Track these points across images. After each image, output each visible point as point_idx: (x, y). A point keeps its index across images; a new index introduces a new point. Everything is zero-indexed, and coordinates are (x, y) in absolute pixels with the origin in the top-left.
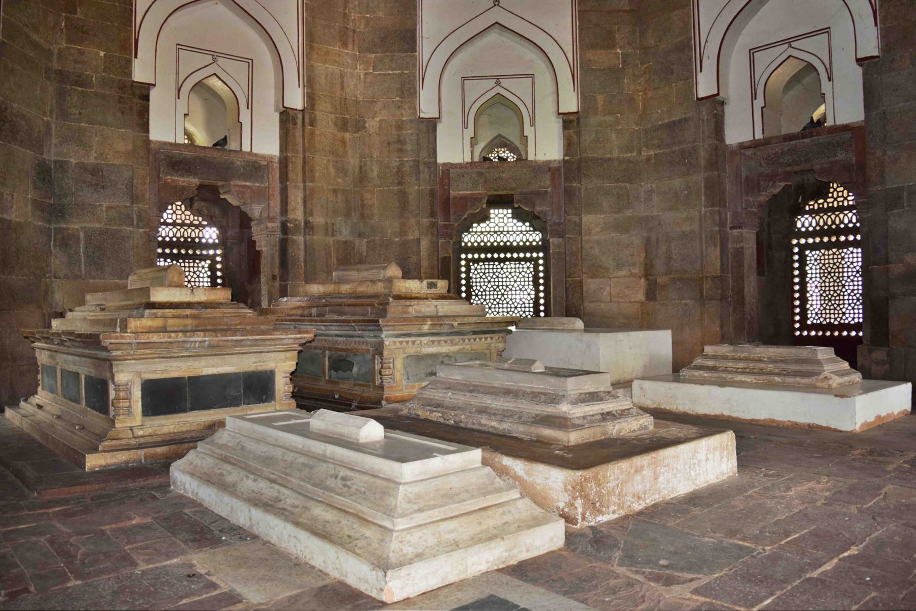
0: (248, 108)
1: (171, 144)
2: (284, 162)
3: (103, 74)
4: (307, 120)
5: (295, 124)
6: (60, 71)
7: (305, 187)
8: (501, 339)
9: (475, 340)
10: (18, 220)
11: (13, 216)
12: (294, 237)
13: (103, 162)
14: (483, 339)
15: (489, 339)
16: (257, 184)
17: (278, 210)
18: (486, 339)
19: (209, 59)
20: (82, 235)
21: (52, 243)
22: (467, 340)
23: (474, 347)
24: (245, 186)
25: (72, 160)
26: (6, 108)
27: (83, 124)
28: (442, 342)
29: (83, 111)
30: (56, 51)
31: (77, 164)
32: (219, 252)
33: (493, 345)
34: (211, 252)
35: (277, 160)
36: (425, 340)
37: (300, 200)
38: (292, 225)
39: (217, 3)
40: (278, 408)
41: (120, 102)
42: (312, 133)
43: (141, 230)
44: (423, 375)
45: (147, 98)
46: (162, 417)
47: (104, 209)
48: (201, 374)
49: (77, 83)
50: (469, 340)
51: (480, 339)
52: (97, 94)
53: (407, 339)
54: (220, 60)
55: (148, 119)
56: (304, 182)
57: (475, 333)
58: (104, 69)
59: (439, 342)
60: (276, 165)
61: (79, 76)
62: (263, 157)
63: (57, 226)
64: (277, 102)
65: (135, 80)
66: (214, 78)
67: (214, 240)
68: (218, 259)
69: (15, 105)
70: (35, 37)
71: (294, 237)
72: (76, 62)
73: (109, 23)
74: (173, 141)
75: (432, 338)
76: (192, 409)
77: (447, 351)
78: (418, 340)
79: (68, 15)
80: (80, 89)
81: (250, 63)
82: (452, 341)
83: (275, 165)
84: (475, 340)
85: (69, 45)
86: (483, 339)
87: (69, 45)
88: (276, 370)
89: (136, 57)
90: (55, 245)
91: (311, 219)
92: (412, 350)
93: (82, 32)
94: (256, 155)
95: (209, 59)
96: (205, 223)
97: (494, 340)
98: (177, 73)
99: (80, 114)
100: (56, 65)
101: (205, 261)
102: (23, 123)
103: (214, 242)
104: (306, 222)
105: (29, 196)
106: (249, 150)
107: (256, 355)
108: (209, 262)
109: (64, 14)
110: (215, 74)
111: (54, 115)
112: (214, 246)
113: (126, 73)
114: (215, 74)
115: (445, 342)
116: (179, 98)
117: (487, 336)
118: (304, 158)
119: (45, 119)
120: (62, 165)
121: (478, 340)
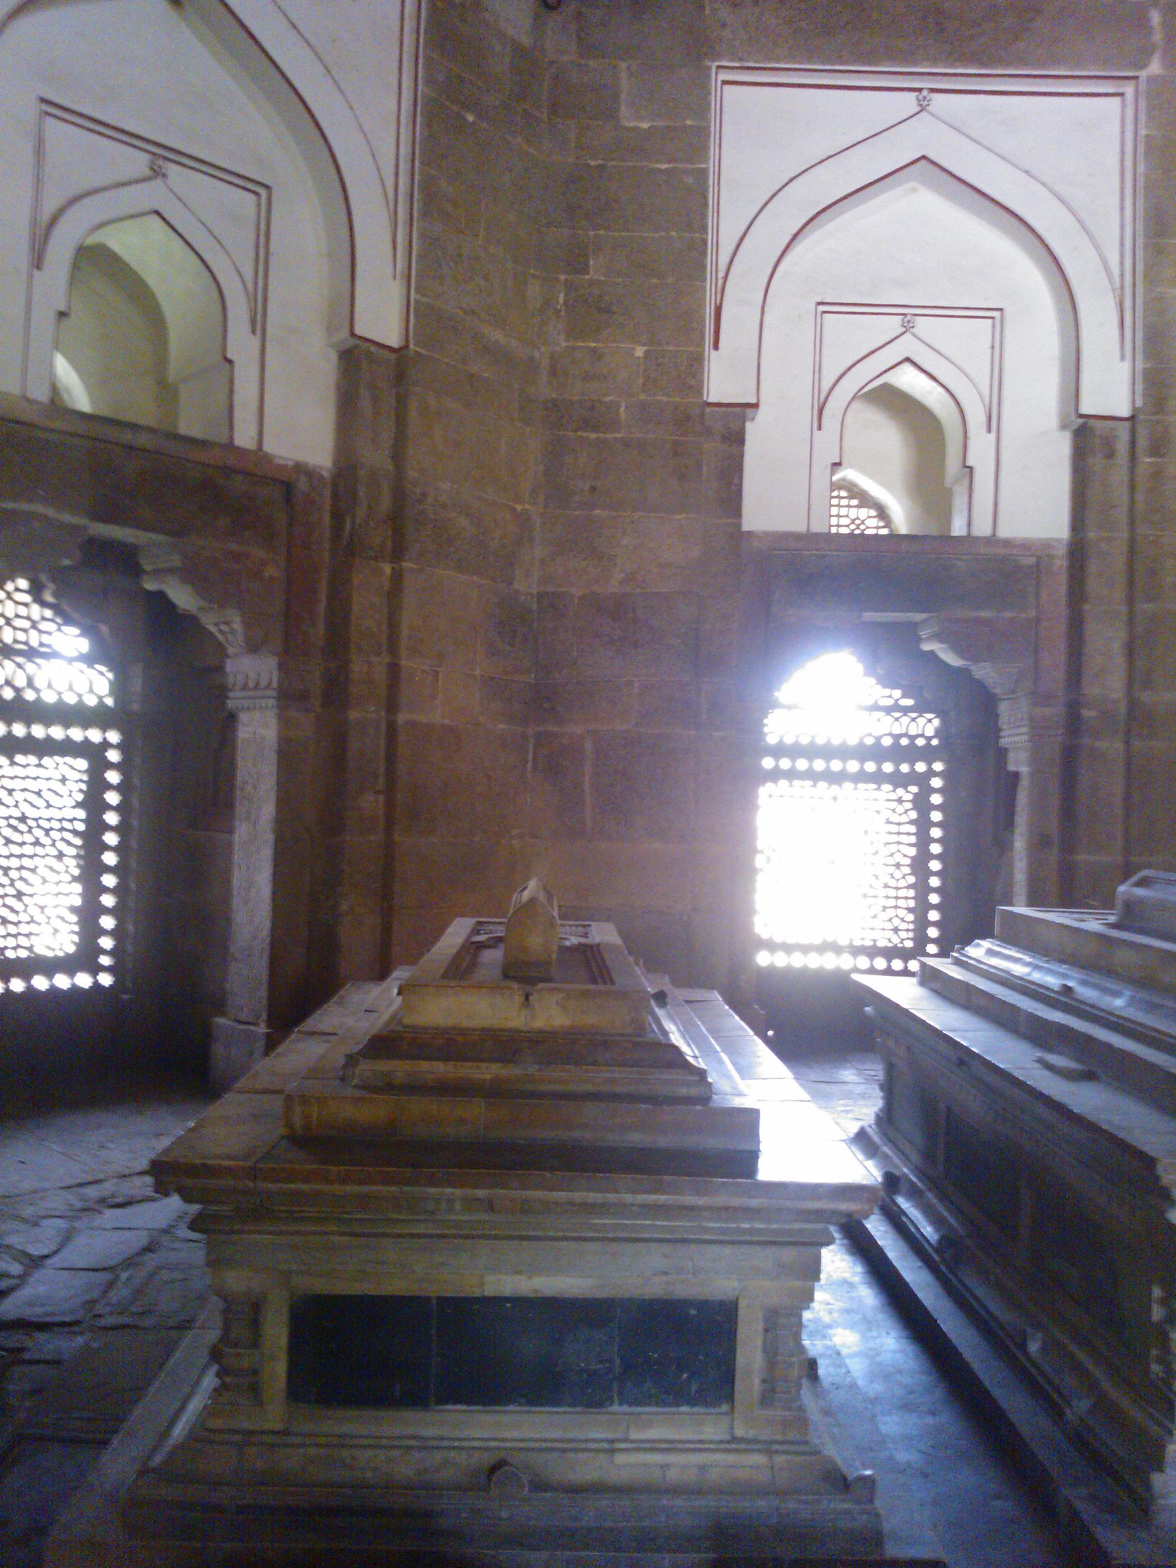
0: (989, 431)
1: (797, 536)
2: (1078, 551)
3: (642, 397)
4: (1142, 442)
5: (1111, 455)
6: (554, 401)
7: (1131, 614)
10: (447, 722)
11: (437, 716)
12: (1099, 744)
13: (639, 590)
16: (1008, 614)
17: (1060, 675)
19: (893, 324)
20: (589, 746)
21: (529, 766)
24: (978, 621)
25: (573, 591)
26: (424, 495)
27: (597, 512)
29: (598, 484)
30: (545, 363)
31: (581, 598)
32: (938, 766)
34: (921, 767)
35: (1061, 551)
37: (1117, 646)
38: (1093, 713)
39: (914, 190)
40: (739, 1433)
41: (676, 454)
42: (1157, 474)
45: (737, 439)
46: (353, 1412)
47: (636, 690)
48: (477, 1293)
49: (586, 424)
52: (627, 444)
54: (923, 325)
55: (740, 486)
56: (1131, 600)
58: (644, 384)
60: (1061, 563)
61: (592, 408)
62: (1026, 546)
63: (541, 729)
64: (1063, 401)
65: (712, 399)
66: (907, 368)
67: (929, 739)
68: (936, 783)
69: (445, 486)
70: (498, 336)
71: (1099, 744)
72: (587, 378)
73: (655, 281)
74: (800, 527)
76: (441, 1401)
79: (570, 278)
80: (593, 436)
81: (995, 314)
83: (1058, 562)
85: (572, 343)
87: (572, 343)
89: (716, 347)
90: (535, 767)
91: (1145, 697)
93: (599, 310)
94: (1007, 543)
95: (893, 324)
96: (909, 702)
98: (818, 369)
99: (593, 489)
100: (544, 389)
101: (905, 787)
102: (463, 522)
103: (928, 745)
104: (1133, 705)
105: (477, 672)
106: (964, 533)
107: (667, 1249)
108: (914, 789)
109: (562, 277)
110: (908, 360)
111: (541, 499)
112: (928, 754)
113: (691, 387)
114: (908, 360)
116: (820, 428)
118: (1132, 542)
119: (519, 507)
120: (552, 603)
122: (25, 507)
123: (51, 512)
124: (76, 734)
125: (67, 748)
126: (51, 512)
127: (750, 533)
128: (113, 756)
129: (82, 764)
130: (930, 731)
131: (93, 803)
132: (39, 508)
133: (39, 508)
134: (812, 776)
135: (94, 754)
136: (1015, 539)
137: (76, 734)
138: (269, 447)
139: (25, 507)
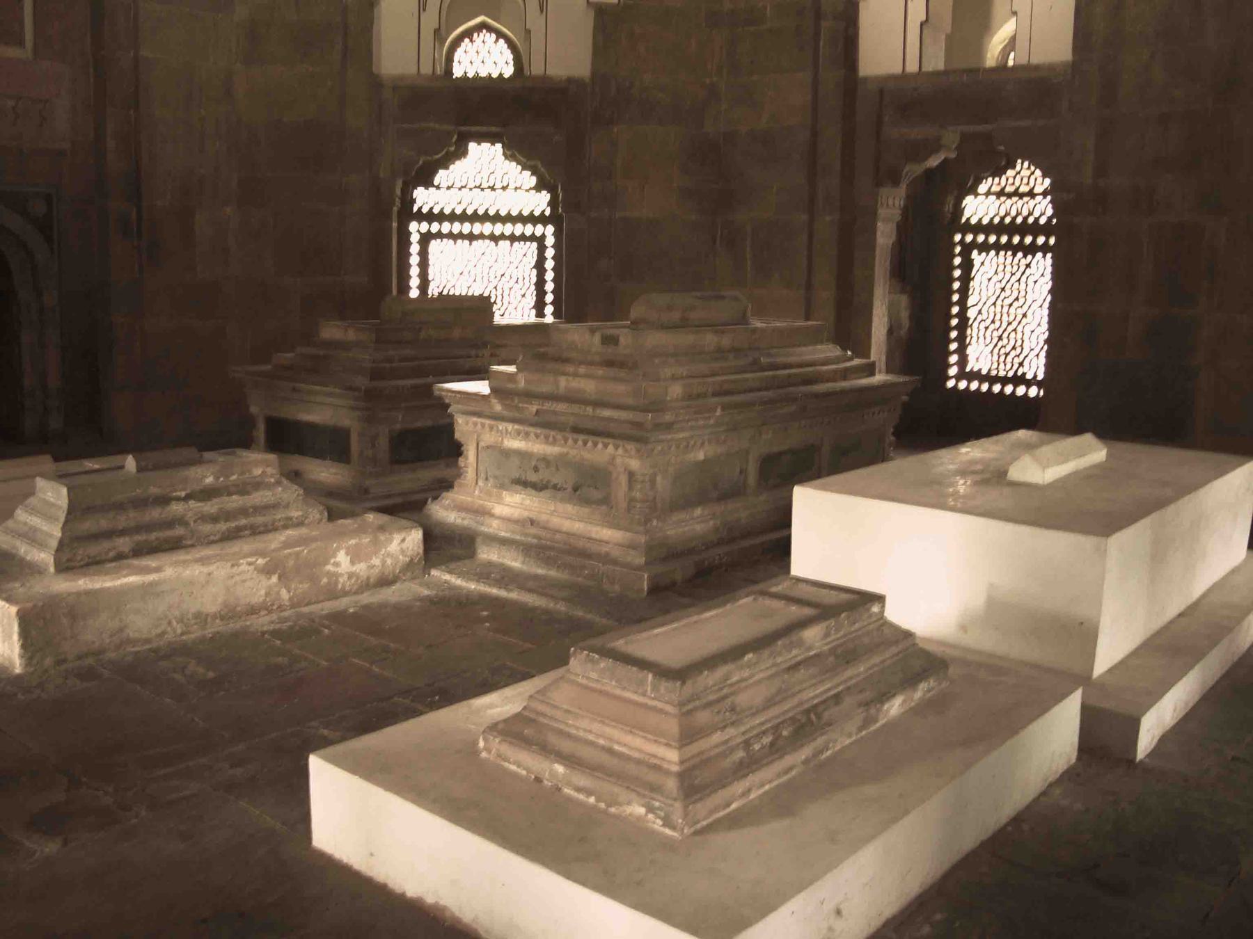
8: (633, 453)
9: (585, 443)
14: (600, 446)
15: (611, 448)
18: (606, 446)
22: (570, 441)
23: (587, 455)
28: (532, 435)
33: (619, 460)
36: (510, 427)
43: (828, 218)
44: (506, 481)
50: (576, 441)
51: (595, 445)
53: (475, 419)
57: (576, 430)
59: (527, 434)
62: (1051, 68)
74: (898, 69)
75: (516, 427)
77: (541, 452)
78: (502, 426)
80: (752, 29)
82: (547, 437)
84: (585, 443)
86: (600, 446)
88: (352, 429)
92: (488, 438)
94: (1037, 68)
97: (620, 451)
115: (537, 436)
117: (606, 440)
119: (708, 81)
121: (590, 444)
122: (424, 125)
123: (437, 126)
124: (529, 230)
125: (523, 238)
126: (437, 126)
127: (866, 79)
128: (550, 241)
129: (535, 245)
130: (1050, 212)
131: (540, 266)
132: (432, 125)
133: (432, 125)
134: (1008, 246)
135: (540, 240)
136: (1044, 64)
137: (529, 230)
138: (550, 72)
139: (424, 125)
